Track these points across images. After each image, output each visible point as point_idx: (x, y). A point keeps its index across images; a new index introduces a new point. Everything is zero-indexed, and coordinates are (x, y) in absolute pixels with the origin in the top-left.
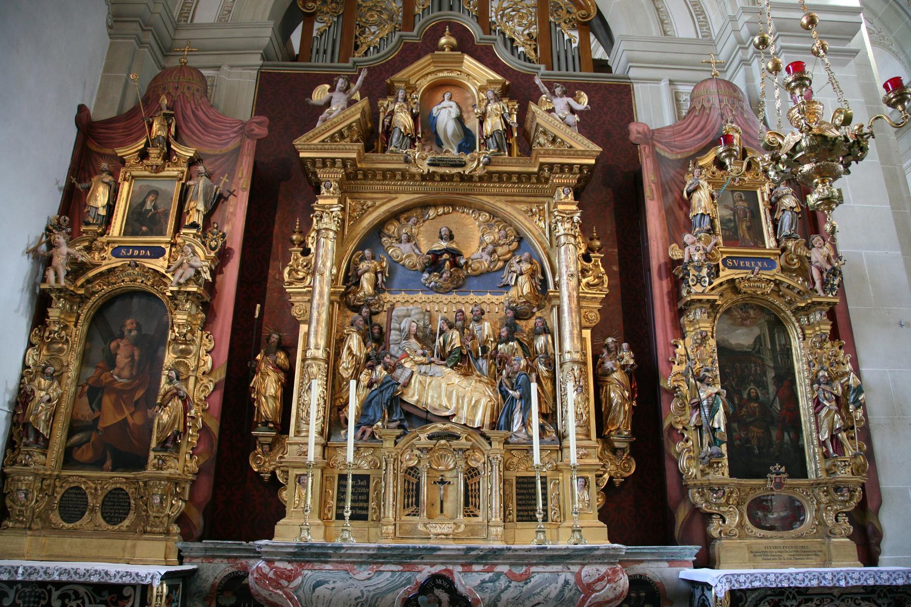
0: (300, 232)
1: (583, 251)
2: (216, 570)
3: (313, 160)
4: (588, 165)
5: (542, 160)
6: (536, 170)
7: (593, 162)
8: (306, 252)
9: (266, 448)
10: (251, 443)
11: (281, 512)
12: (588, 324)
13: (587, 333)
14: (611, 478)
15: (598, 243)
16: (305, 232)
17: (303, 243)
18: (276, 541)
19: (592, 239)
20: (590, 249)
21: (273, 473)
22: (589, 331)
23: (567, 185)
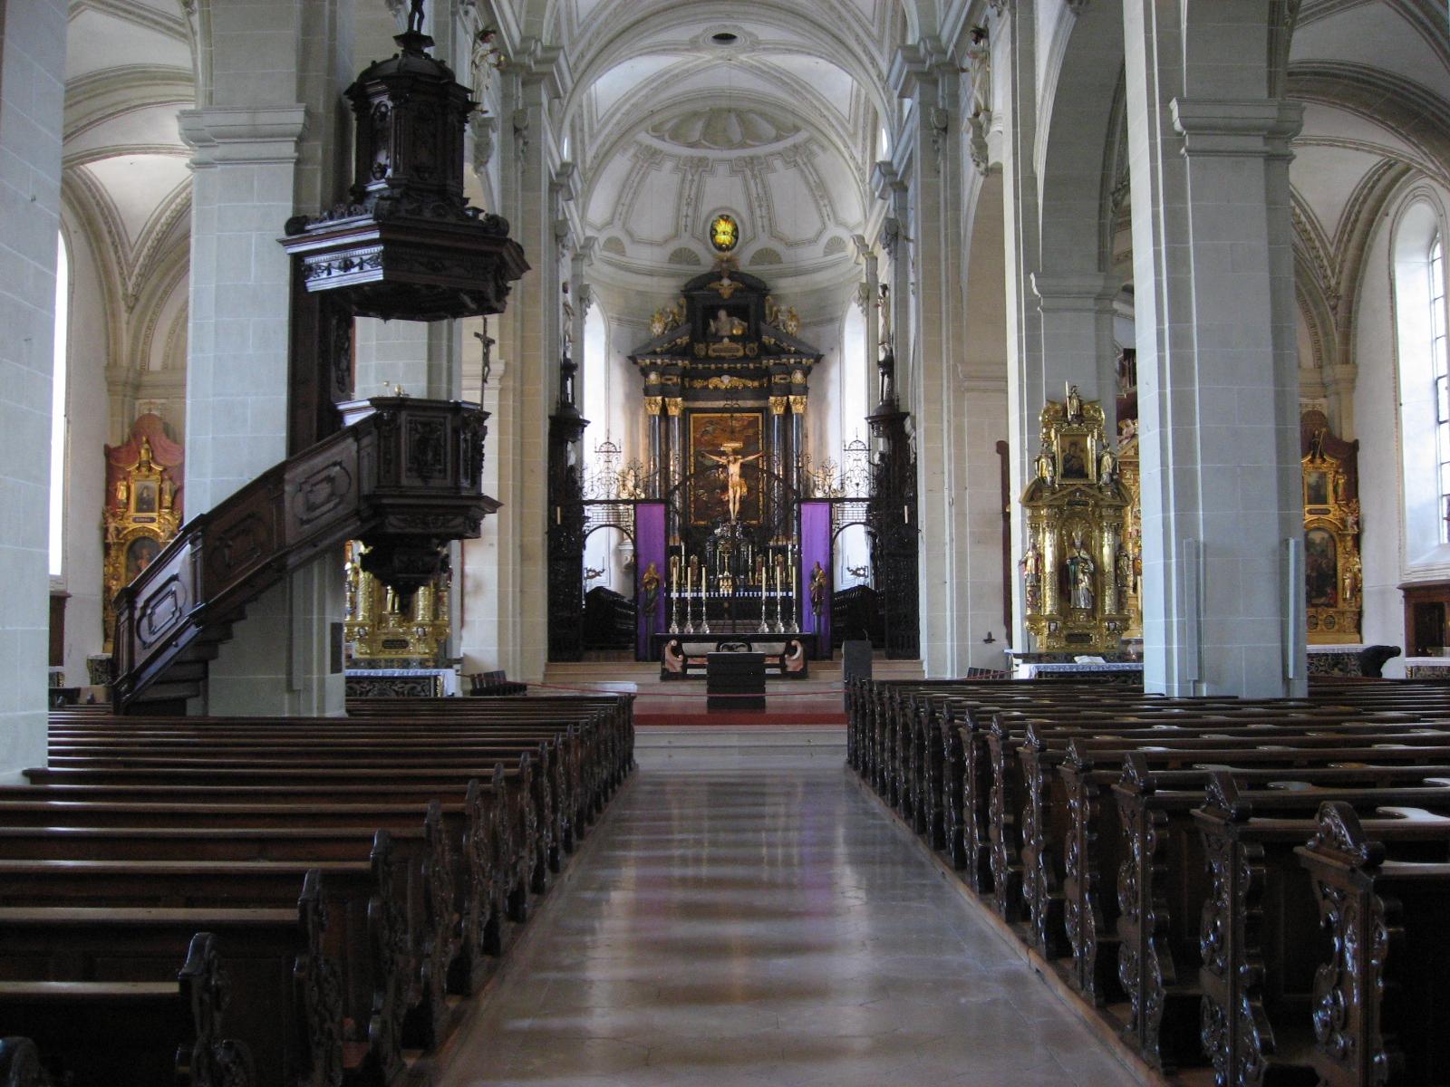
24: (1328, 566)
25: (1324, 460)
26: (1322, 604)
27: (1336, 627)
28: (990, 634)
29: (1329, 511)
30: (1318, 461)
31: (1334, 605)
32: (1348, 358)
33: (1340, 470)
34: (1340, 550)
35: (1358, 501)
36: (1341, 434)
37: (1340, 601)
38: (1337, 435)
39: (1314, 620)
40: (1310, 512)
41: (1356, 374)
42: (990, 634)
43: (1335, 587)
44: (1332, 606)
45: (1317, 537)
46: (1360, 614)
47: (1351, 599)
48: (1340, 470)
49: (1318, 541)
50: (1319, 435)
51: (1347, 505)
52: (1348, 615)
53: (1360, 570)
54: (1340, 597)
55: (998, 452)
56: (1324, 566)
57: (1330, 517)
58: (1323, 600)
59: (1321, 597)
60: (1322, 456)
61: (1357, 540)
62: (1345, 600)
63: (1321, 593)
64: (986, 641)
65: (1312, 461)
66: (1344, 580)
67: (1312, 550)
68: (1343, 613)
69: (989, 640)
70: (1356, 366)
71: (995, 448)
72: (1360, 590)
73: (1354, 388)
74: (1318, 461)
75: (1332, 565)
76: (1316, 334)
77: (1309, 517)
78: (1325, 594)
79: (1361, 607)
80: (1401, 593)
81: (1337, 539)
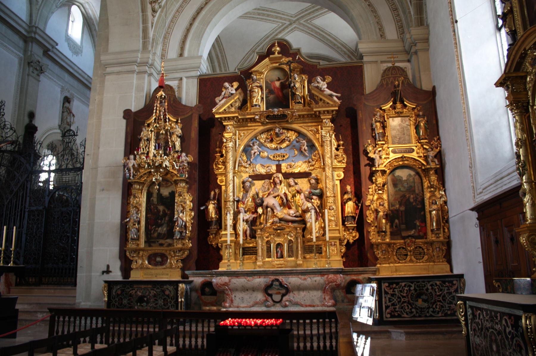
0: (219, 148)
1: (336, 146)
2: (198, 280)
3: (221, 118)
4: (336, 110)
5: (315, 110)
6: (313, 113)
7: (337, 108)
8: (222, 156)
9: (214, 235)
10: (207, 234)
11: (220, 258)
12: (338, 178)
13: (338, 183)
14: (348, 241)
15: (342, 142)
16: (221, 147)
17: (221, 152)
18: (220, 269)
19: (340, 140)
20: (339, 145)
21: (217, 244)
22: (339, 181)
23: (328, 119)
24: (415, 201)
25: (405, 106)
26: (412, 236)
27: (426, 257)
28: (108, 266)
29: (413, 150)
30: (399, 105)
31: (425, 236)
32: (422, 22)
33: (421, 113)
34: (426, 184)
35: (439, 139)
36: (421, 86)
37: (429, 233)
38: (419, 87)
39: (403, 252)
40: (394, 152)
41: (428, 34)
42: (108, 266)
43: (424, 220)
44: (422, 238)
45: (403, 174)
46: (448, 244)
47: (438, 229)
48: (421, 113)
49: (404, 178)
50: (399, 85)
51: (428, 143)
52: (436, 245)
53: (445, 203)
54: (429, 229)
55: (124, 118)
56: (412, 200)
57: (414, 155)
58: (413, 232)
59: (412, 229)
60: (402, 102)
61: (441, 172)
62: (432, 231)
63: (410, 226)
64: (103, 272)
65: (394, 107)
66: (430, 212)
67: (400, 186)
68: (432, 243)
69: (108, 272)
70: (428, 26)
71: (122, 114)
72: (447, 221)
73: (429, 46)
74: (399, 105)
75: (420, 199)
76: (398, 15)
77: (392, 156)
78: (414, 227)
79: (449, 237)
80: (475, 214)
81: (422, 175)
